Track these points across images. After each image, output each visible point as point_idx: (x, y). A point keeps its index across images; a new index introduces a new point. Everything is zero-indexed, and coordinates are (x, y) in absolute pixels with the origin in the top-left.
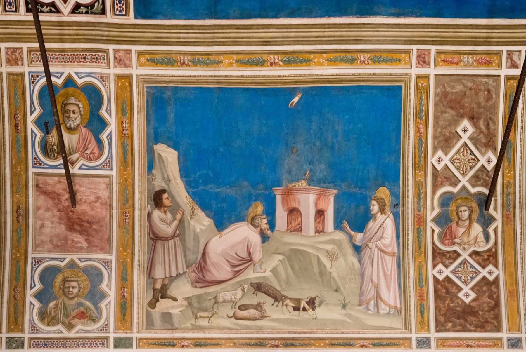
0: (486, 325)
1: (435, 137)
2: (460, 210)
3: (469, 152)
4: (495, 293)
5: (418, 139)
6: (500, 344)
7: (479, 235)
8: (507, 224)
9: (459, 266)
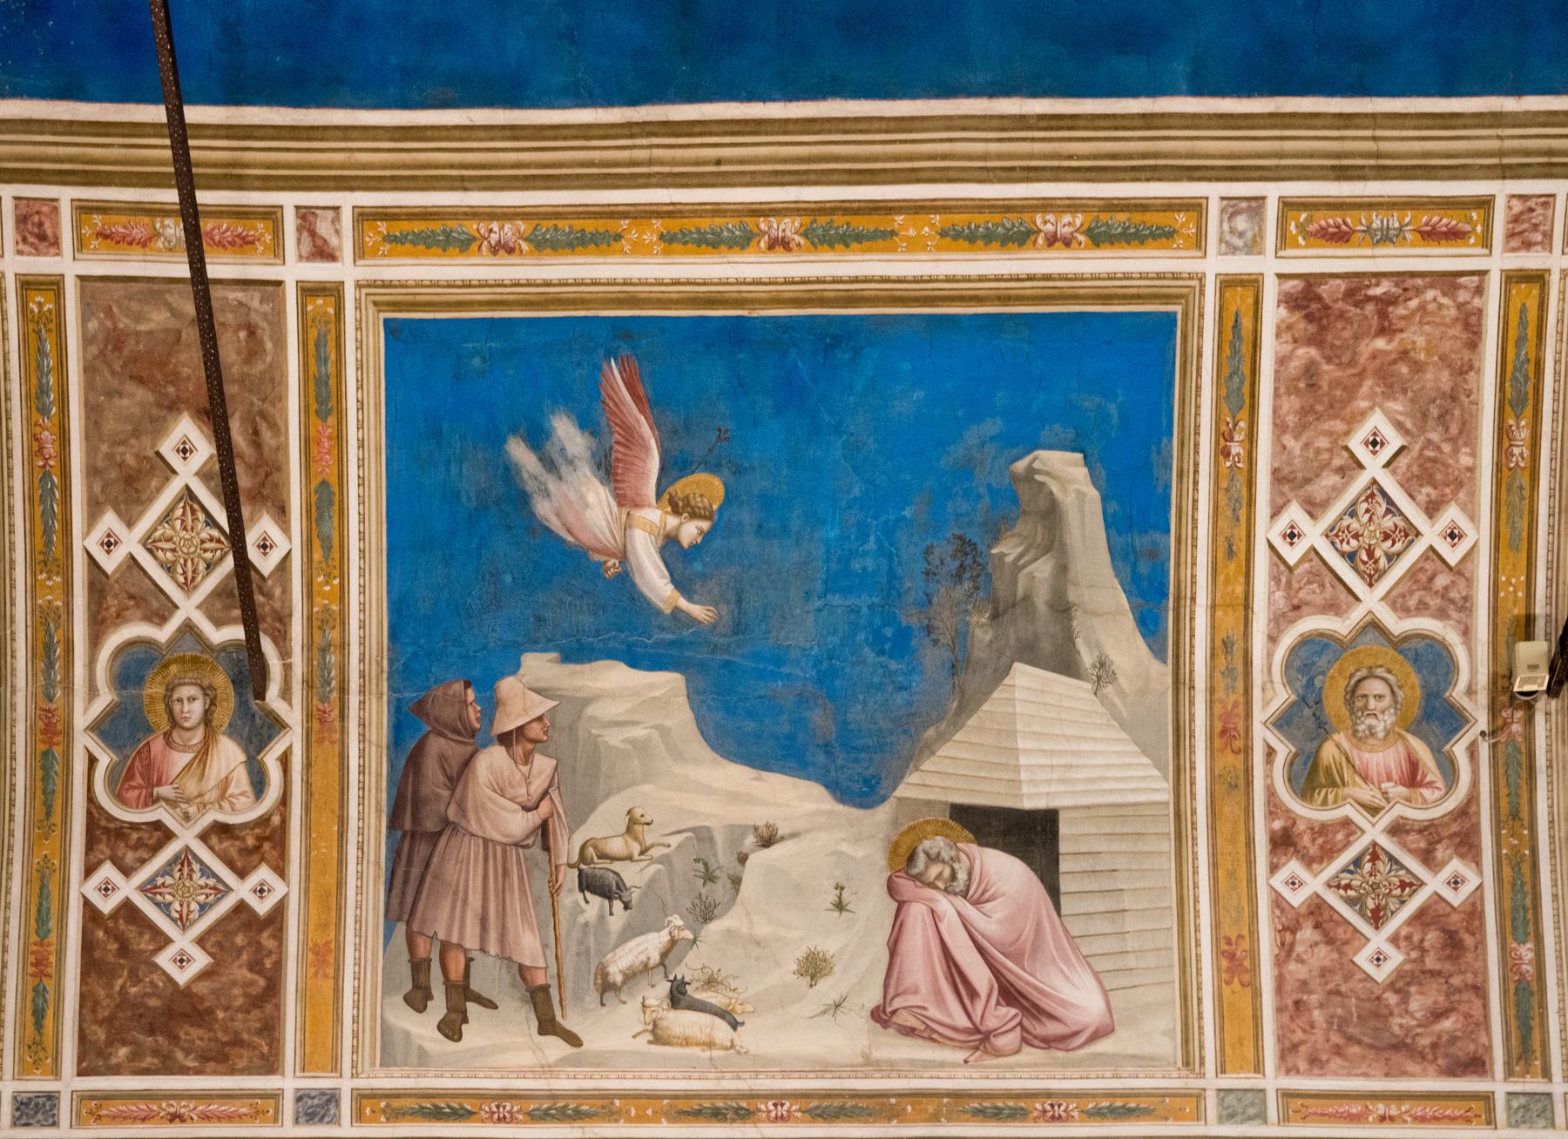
0: (234, 1052)
1: (92, 472)
2: (175, 696)
3: (201, 516)
4: (270, 953)
5: (38, 475)
6: (271, 1112)
7: (235, 774)
8: (321, 741)
9: (166, 870)
